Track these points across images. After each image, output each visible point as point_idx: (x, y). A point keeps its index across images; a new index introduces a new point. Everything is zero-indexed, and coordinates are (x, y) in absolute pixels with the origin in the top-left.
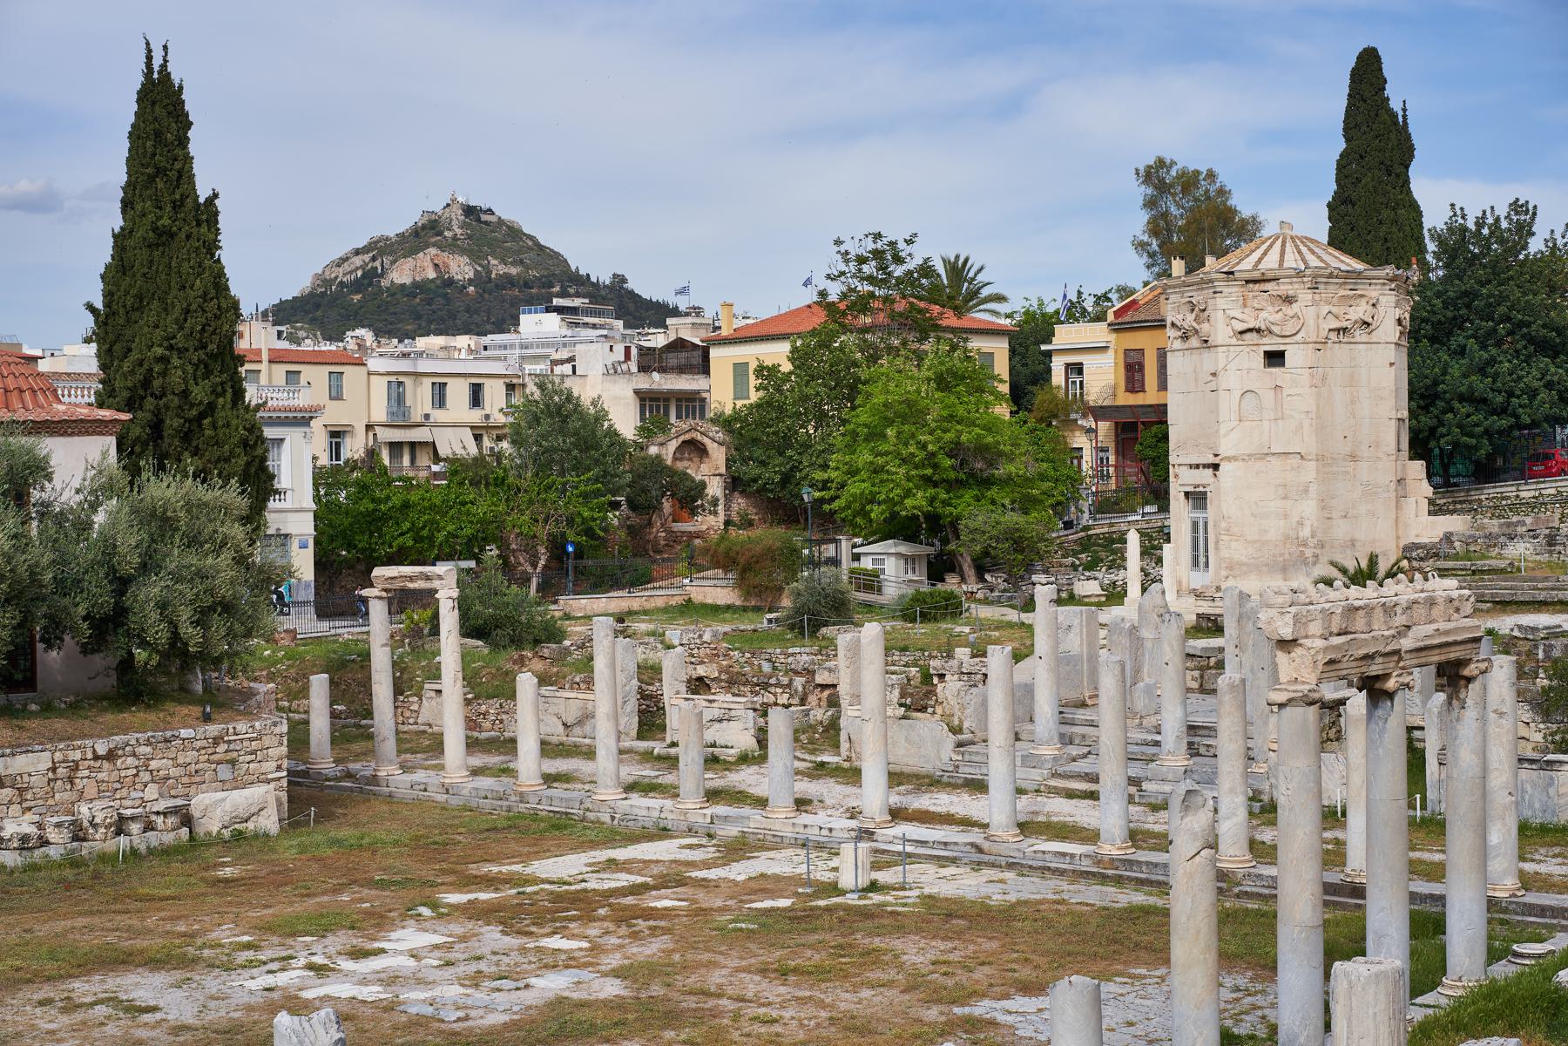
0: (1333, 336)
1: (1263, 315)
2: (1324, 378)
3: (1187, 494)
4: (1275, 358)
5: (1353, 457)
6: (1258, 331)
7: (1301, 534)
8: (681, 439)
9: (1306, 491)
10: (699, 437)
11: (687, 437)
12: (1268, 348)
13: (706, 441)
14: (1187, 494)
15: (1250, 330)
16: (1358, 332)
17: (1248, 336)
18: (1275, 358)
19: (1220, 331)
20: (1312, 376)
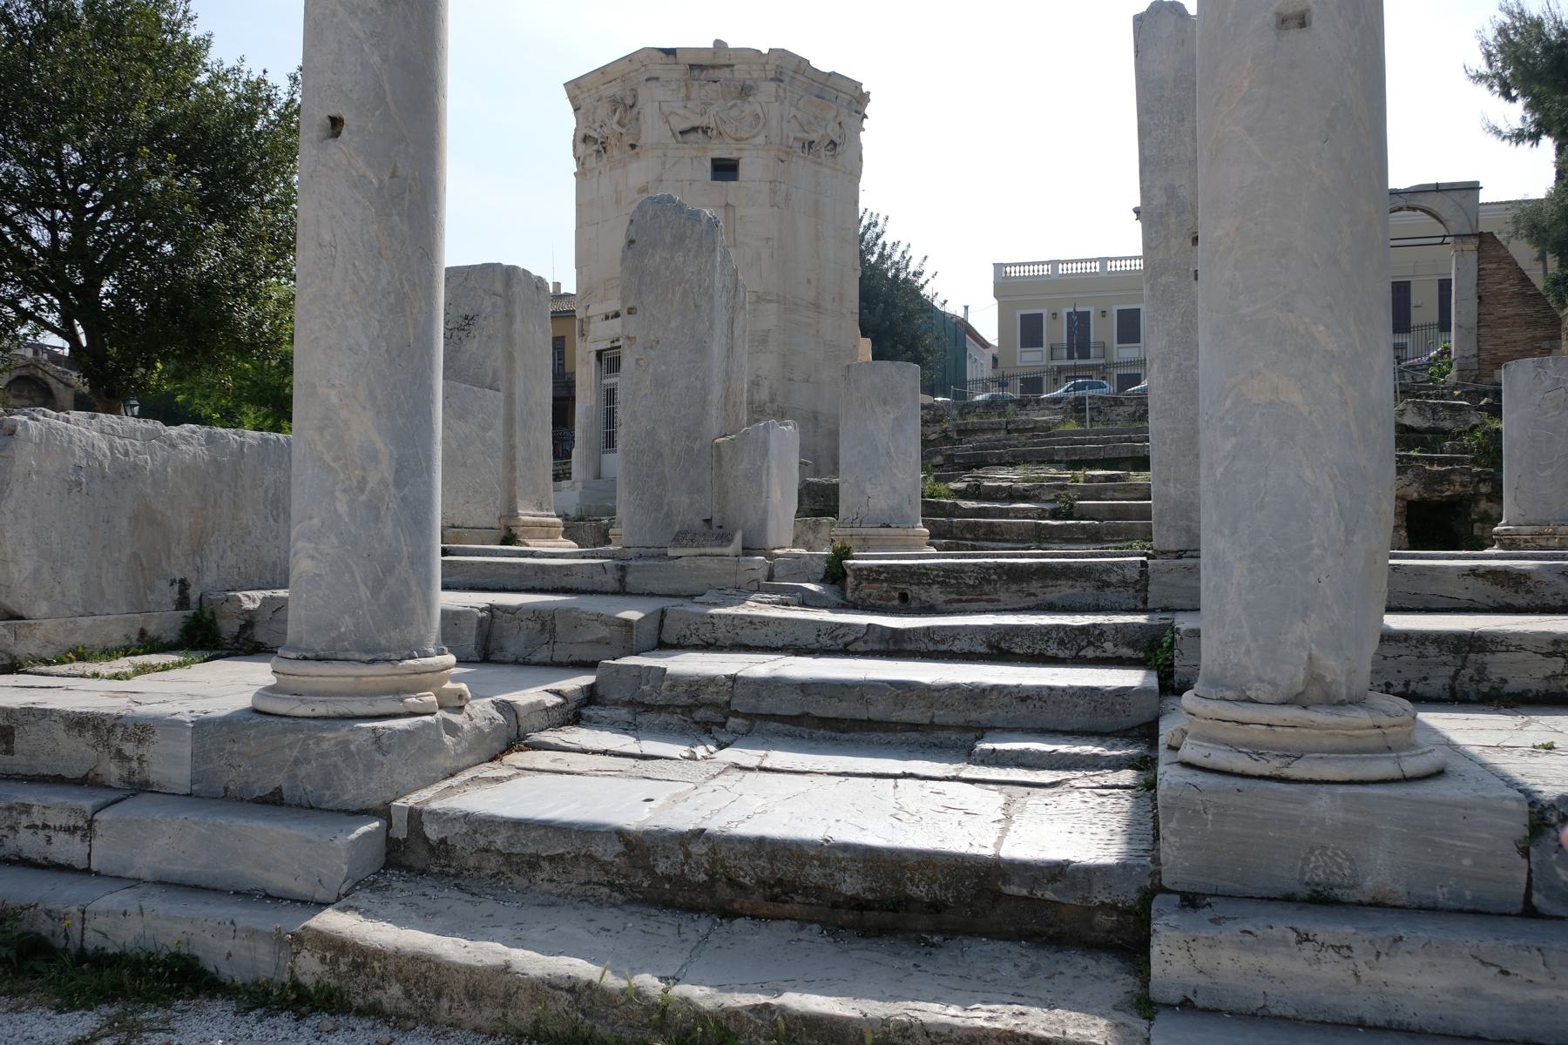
0: (798, 145)
1: (712, 110)
2: (787, 199)
3: (599, 354)
4: (725, 169)
5: (816, 306)
6: (705, 130)
7: (756, 397)
8: (15, 374)
9: (764, 341)
10: (40, 374)
11: (24, 372)
12: (717, 154)
13: (51, 381)
14: (599, 354)
15: (694, 129)
16: (823, 152)
17: (691, 137)
18: (725, 169)
19: (652, 128)
20: (773, 192)
